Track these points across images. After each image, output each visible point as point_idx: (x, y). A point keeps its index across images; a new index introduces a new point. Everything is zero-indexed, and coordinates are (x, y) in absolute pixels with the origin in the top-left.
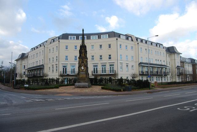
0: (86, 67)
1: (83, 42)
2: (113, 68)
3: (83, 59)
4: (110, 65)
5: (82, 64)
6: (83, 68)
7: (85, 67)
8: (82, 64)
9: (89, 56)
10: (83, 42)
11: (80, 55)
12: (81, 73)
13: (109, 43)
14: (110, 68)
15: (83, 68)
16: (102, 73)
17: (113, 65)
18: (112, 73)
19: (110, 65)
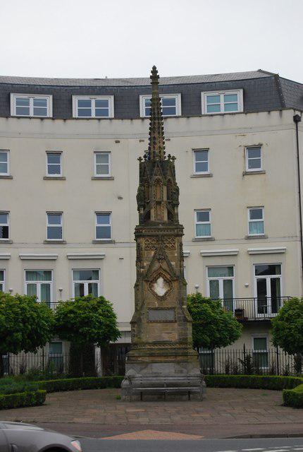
0: (176, 278)
1: (156, 132)
2: (275, 283)
3: (159, 239)
4: (260, 270)
5: (157, 265)
6: (160, 288)
7: (175, 284)
8: (157, 265)
9: (186, 216)
10: (156, 132)
11: (145, 218)
12: (154, 315)
13: (253, 140)
14: (261, 285)
15: (160, 288)
16: (260, 311)
17: (273, 269)
18: (270, 314)
19: (260, 270)
